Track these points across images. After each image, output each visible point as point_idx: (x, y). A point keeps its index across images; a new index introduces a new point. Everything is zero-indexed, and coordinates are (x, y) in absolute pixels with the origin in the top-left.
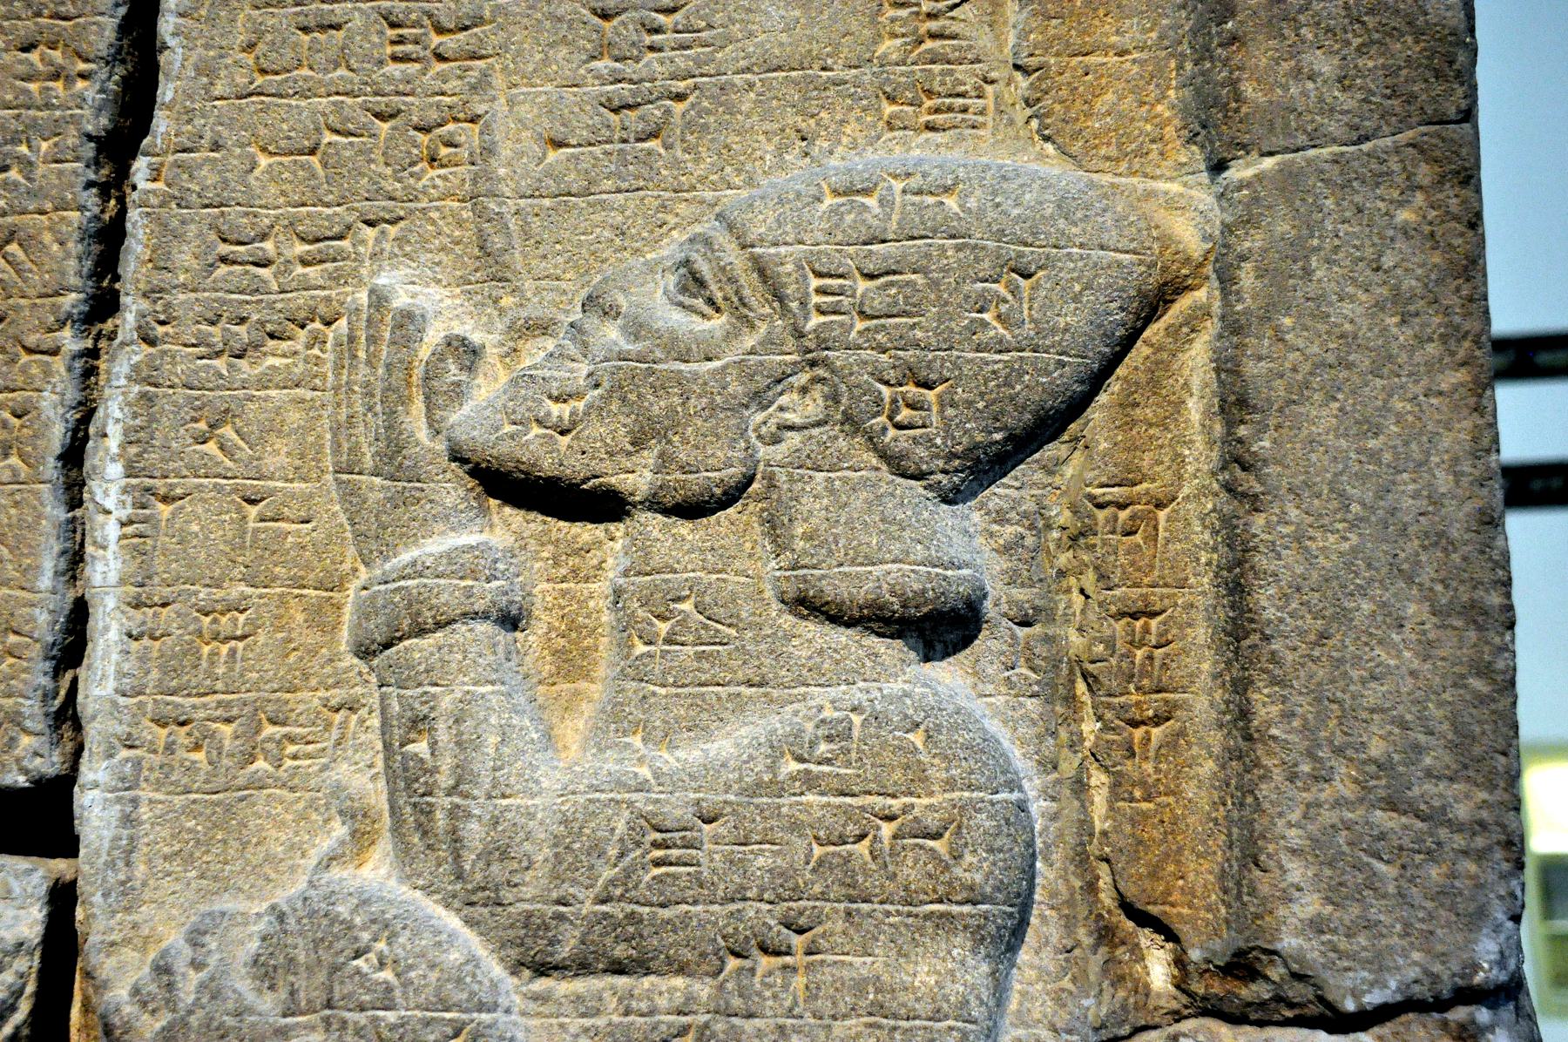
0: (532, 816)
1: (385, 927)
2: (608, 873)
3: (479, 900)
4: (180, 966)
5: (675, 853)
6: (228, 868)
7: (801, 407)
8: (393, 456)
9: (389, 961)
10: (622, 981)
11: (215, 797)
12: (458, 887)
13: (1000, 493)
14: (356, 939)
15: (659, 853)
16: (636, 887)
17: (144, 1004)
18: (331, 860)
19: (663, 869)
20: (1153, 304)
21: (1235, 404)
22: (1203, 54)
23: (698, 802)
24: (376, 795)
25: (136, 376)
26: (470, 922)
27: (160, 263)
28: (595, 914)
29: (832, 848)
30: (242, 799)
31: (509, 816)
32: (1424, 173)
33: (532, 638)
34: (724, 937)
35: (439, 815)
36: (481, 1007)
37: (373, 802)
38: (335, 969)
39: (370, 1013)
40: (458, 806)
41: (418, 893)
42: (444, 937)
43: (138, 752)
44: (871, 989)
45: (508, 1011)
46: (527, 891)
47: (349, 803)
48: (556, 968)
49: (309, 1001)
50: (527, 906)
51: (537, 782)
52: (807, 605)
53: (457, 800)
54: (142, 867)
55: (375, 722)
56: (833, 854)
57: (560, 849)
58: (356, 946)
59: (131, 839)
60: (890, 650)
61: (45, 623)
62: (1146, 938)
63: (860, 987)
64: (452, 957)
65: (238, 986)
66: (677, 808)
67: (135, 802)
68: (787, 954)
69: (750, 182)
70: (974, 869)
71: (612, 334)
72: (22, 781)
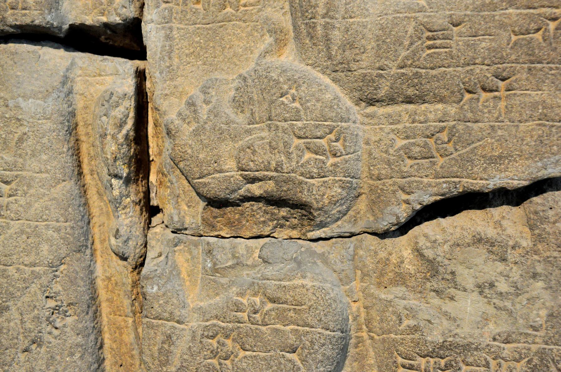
0: (365, 27)
1: (295, 82)
2: (404, 53)
3: (339, 69)
4: (199, 102)
5: (438, 42)
6: (216, 59)
9: (297, 98)
10: (411, 107)
11: (208, 26)
12: (329, 63)
14: (281, 88)
15: (431, 43)
16: (418, 60)
17: (184, 120)
19: (433, 51)
23: (451, 16)
24: (287, 22)
26: (334, 80)
28: (398, 74)
29: (522, 36)
30: (221, 27)
31: (353, 27)
34: (463, 83)
35: (319, 28)
36: (342, 120)
37: (285, 25)
38: (272, 102)
39: (289, 122)
40: (328, 23)
41: (309, 67)
42: (323, 87)
43: (170, 5)
44: (540, 107)
45: (354, 122)
46: (364, 64)
47: (273, 26)
48: (378, 101)
49: (260, 118)
50: (364, 71)
51: (367, 10)
53: (328, 20)
54: (176, 60)
56: (523, 39)
57: (380, 42)
58: (281, 91)
59: (170, 46)
63: (534, 106)
64: (327, 97)
65: (227, 111)
67: (171, 29)
68: (496, 91)
72: (118, 20)
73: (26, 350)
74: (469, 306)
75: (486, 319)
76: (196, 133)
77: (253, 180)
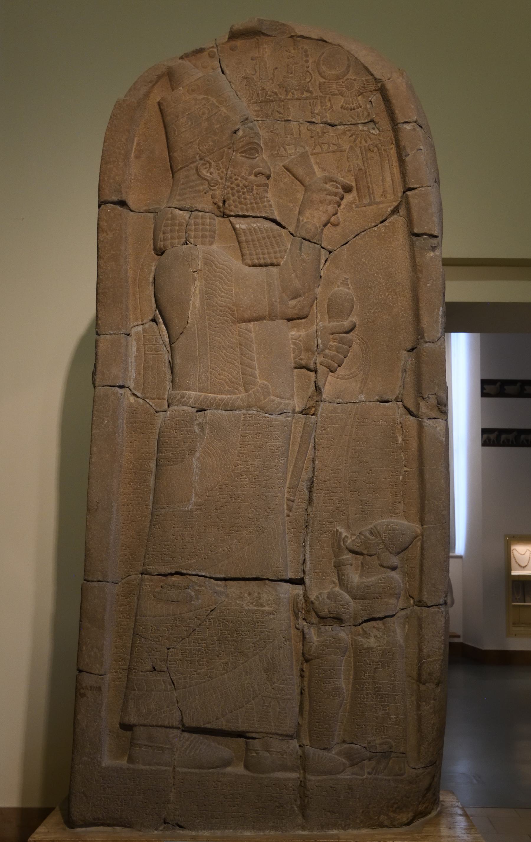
3: (349, 593)
7: (382, 547)
8: (339, 547)
13: (400, 555)
18: (333, 587)
20: (415, 538)
21: (422, 549)
24: (337, 581)
25: (311, 536)
32: (441, 528)
33: (353, 566)
52: (382, 566)
60: (389, 570)
61: (301, 561)
62: (411, 599)
69: (376, 521)
70: (396, 591)
71: (363, 537)
74: (372, 640)
76: (319, 604)
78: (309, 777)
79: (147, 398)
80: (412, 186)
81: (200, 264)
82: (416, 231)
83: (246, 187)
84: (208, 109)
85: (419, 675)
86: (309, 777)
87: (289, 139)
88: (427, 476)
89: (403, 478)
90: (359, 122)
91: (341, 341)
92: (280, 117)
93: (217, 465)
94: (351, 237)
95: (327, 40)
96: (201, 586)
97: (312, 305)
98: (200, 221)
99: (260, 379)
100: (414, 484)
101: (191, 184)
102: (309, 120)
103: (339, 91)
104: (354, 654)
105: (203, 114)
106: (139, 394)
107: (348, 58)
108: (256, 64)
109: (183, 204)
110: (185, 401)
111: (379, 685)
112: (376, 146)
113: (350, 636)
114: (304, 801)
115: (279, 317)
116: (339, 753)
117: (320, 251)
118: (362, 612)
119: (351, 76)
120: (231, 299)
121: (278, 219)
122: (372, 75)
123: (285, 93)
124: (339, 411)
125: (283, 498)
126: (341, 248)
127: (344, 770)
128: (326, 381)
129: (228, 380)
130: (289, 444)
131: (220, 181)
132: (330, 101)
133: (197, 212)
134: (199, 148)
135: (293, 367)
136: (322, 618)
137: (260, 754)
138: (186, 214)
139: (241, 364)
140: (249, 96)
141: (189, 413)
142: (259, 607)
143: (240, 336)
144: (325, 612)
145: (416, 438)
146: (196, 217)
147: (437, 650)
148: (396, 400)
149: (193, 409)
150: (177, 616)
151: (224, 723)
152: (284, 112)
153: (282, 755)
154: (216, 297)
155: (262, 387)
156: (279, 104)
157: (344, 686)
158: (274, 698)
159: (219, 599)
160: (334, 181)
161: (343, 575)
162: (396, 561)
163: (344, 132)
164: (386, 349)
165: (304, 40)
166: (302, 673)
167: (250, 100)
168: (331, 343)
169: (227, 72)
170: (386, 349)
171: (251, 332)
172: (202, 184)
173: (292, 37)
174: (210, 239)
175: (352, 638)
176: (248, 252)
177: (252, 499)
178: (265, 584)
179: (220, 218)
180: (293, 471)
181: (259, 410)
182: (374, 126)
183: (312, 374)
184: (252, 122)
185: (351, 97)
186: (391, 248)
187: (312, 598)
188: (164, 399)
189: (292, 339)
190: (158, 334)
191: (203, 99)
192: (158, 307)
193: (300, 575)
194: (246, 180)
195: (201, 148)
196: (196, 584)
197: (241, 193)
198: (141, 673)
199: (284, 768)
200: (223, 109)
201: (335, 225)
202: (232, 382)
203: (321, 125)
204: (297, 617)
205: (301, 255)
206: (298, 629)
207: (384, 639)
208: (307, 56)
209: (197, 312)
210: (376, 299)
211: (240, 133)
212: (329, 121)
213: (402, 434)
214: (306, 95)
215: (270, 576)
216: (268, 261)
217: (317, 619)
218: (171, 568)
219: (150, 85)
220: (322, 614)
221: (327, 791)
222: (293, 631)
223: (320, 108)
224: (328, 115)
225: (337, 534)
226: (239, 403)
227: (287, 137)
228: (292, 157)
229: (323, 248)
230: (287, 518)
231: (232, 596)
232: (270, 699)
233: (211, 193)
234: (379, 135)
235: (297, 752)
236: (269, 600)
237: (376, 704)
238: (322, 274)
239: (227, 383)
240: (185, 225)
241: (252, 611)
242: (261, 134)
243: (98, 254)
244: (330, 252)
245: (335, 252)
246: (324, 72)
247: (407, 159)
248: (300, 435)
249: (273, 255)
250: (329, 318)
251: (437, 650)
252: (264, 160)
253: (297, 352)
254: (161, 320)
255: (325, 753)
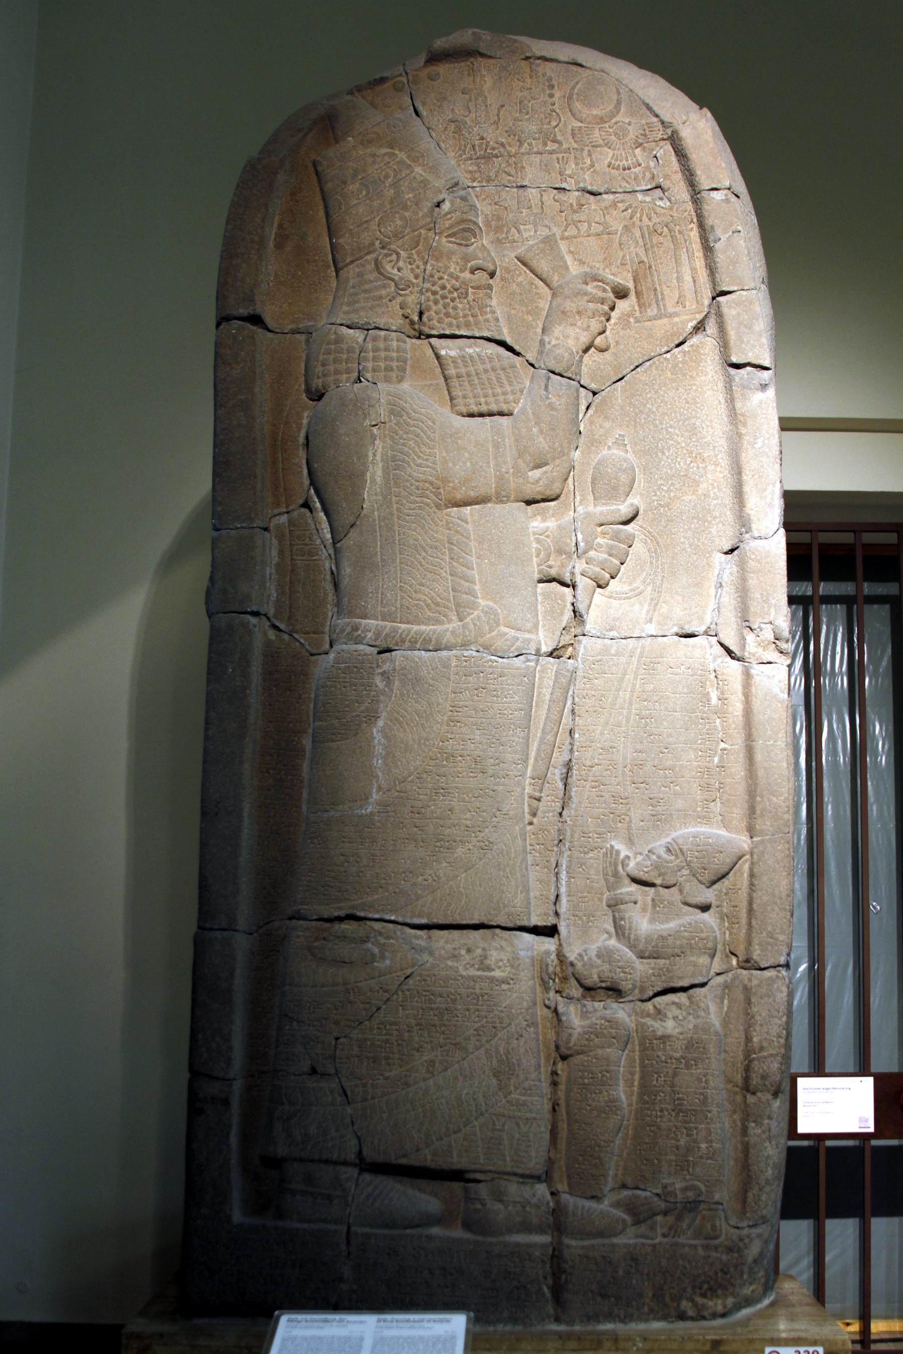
1: (618, 950)
2: (653, 944)
3: (632, 947)
7: (685, 872)
8: (616, 874)
18: (606, 940)
20: (740, 858)
21: (752, 875)
22: (750, 819)
24: (612, 930)
25: (568, 856)
27: (572, 836)
32: (782, 841)
33: (638, 906)
55: (611, 918)
60: (698, 911)
61: (553, 898)
62: (733, 957)
66: (665, 934)
70: (710, 945)
71: (654, 857)
73: (517, 1039)
75: (675, 1027)
76: (584, 965)
77: (602, 982)
78: (567, 1241)
79: (297, 632)
80: (725, 289)
81: (383, 411)
82: (734, 359)
83: (456, 290)
84: (395, 170)
85: (747, 1079)
86: (567, 1241)
87: (524, 214)
88: (759, 757)
89: (720, 761)
90: (638, 189)
91: (616, 537)
92: (509, 181)
93: (413, 740)
94: (628, 370)
95: (584, 64)
96: (388, 938)
97: (566, 479)
98: (382, 345)
99: (483, 598)
100: (738, 770)
101: (367, 287)
102: (557, 186)
103: (603, 140)
104: (640, 1045)
105: (387, 177)
106: (282, 626)
107: (617, 90)
108: (470, 100)
109: (354, 318)
110: (359, 635)
111: (681, 1095)
112: (667, 226)
113: (633, 1018)
114: (559, 1279)
115: (512, 498)
116: (617, 1205)
117: (578, 391)
118: (653, 978)
119: (622, 117)
120: (434, 469)
121: (509, 341)
122: (657, 116)
123: (518, 144)
124: (613, 651)
125: (523, 793)
126: (613, 387)
127: (624, 1230)
128: (591, 602)
129: (430, 601)
130: (531, 706)
131: (414, 281)
132: (590, 155)
133: (376, 331)
134: (380, 231)
135: (536, 579)
136: (589, 990)
137: (488, 1206)
138: (359, 335)
139: (451, 575)
140: (460, 149)
141: (366, 655)
142: (484, 971)
143: (449, 529)
144: (593, 978)
145: (740, 695)
146: (375, 339)
147: (775, 1039)
148: (706, 633)
149: (373, 649)
150: (349, 986)
151: (429, 1157)
152: (516, 173)
153: (524, 1207)
154: (409, 466)
155: (486, 612)
156: (507, 161)
157: (623, 1097)
158: (510, 1117)
159: (419, 958)
160: (599, 281)
161: (622, 919)
162: (708, 896)
163: (614, 205)
164: (689, 550)
165: (547, 63)
166: (555, 1077)
167: (461, 156)
168: (599, 540)
169: (424, 113)
170: (689, 550)
171: (467, 523)
172: (384, 286)
173: (527, 58)
174: (400, 374)
175: (636, 1020)
176: (460, 394)
177: (470, 795)
178: (494, 935)
179: (414, 341)
180: (538, 750)
181: (481, 650)
182: (662, 195)
183: (568, 591)
184: (465, 189)
185: (624, 149)
186: (694, 388)
187: (572, 956)
188: (323, 633)
189: (534, 533)
190: (313, 527)
191: (385, 154)
192: (313, 483)
193: (550, 921)
194: (457, 278)
195: (382, 230)
196: (380, 934)
197: (448, 300)
198: (293, 1077)
199: (527, 1227)
200: (418, 170)
201: (602, 351)
202: (437, 604)
203: (577, 193)
204: (547, 989)
205: (547, 398)
206: (548, 1007)
207: (689, 1021)
208: (552, 87)
209: (378, 490)
210: (671, 469)
211: (446, 206)
212: (589, 188)
213: (717, 688)
214: (551, 146)
215: (502, 920)
216: (494, 408)
217: (581, 990)
218: (340, 908)
219: (300, 135)
220: (588, 982)
221: (596, 1263)
222: (541, 1013)
223: (573, 166)
224: (586, 177)
225: (612, 853)
226: (448, 638)
227: (522, 213)
228: (531, 243)
229: (582, 386)
230: (529, 828)
231: (440, 955)
232: (503, 1119)
233: (399, 299)
234: (671, 208)
235: (548, 1203)
236: (501, 960)
237: (675, 1126)
238: (582, 429)
239: (428, 606)
240: (357, 351)
241: (473, 978)
242: (478, 206)
243: (215, 399)
244: (594, 394)
245: (603, 393)
246: (580, 112)
247: (718, 246)
248: (550, 690)
249: (501, 398)
250: (595, 499)
251: (775, 1039)
252: (485, 247)
253: (542, 555)
254: (318, 505)
255: (592, 1204)
